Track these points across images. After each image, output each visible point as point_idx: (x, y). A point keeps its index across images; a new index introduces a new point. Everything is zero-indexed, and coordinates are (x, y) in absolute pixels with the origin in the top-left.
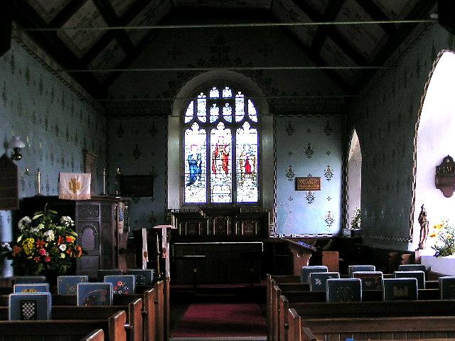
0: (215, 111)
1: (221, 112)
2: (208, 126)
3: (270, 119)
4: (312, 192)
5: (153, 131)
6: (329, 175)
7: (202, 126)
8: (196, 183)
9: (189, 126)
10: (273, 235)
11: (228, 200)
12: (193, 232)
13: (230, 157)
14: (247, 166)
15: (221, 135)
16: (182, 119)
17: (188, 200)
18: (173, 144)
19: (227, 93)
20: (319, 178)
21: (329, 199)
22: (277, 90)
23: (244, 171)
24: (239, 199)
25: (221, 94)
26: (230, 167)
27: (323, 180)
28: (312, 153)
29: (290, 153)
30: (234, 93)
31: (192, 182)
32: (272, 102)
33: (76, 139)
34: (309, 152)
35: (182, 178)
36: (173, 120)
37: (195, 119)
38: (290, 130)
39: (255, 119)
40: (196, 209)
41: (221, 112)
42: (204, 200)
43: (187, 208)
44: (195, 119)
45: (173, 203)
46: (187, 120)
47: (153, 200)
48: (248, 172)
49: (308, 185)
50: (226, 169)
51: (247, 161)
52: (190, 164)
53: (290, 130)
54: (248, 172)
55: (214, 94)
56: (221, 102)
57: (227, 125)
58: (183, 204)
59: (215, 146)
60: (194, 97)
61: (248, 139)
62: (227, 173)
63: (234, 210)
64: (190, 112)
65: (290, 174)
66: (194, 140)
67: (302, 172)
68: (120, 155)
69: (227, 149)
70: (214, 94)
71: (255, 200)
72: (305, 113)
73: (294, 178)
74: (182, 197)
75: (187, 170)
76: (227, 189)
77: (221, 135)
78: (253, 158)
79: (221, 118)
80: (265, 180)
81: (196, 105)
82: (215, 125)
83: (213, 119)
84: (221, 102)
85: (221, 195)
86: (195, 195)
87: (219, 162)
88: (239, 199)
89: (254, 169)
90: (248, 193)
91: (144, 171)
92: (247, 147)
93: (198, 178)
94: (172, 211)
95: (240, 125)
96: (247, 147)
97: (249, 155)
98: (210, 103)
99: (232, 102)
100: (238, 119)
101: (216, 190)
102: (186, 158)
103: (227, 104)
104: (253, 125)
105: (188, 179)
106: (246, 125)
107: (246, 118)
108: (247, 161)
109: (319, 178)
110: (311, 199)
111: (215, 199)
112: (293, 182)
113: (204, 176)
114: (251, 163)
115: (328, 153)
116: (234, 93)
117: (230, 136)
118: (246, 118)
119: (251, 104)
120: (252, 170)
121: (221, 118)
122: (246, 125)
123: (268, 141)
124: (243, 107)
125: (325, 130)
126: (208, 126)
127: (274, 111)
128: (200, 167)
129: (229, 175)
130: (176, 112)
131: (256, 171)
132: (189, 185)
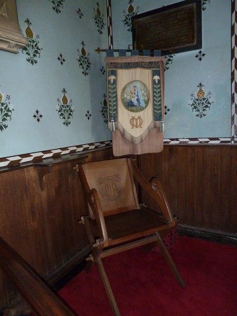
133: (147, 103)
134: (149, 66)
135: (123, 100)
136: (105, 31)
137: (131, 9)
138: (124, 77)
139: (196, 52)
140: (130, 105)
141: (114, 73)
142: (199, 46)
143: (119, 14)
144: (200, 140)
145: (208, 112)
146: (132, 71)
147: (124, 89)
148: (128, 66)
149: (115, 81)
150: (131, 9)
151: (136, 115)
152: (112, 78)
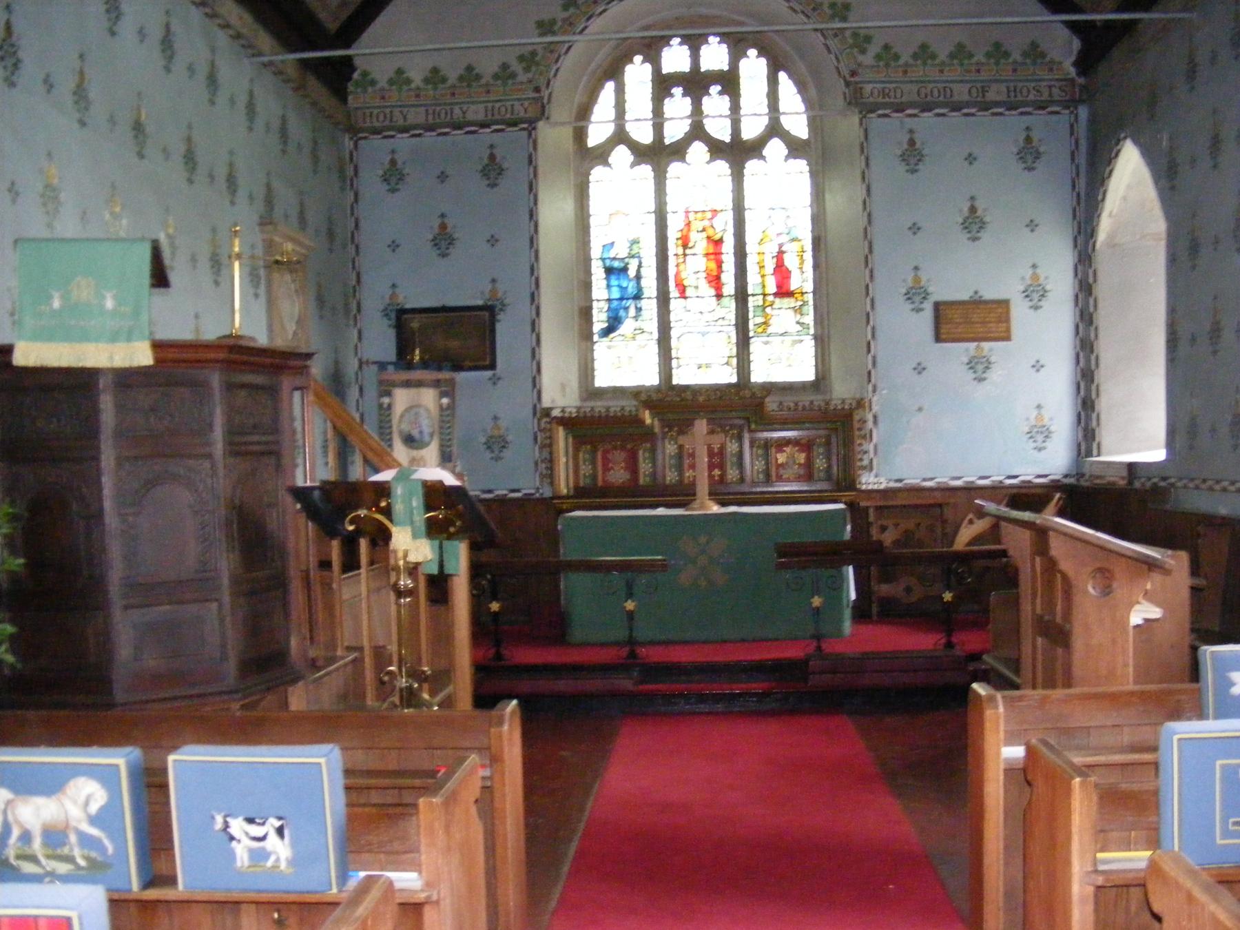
0: (678, 105)
1: (697, 110)
2: (659, 155)
3: (849, 126)
4: (986, 345)
5: (492, 170)
6: (1036, 293)
7: (642, 154)
8: (627, 326)
9: (601, 155)
10: (869, 481)
11: (727, 376)
12: (619, 475)
13: (728, 248)
14: (781, 271)
15: (699, 181)
17: (602, 380)
18: (554, 210)
19: (715, 56)
20: (1004, 304)
21: (1038, 366)
22: (868, 39)
23: (771, 287)
24: (759, 375)
26: (729, 278)
27: (1020, 312)
28: (982, 225)
29: (915, 229)
30: (736, 55)
32: (853, 73)
33: (231, 181)
34: (973, 223)
36: (553, 136)
37: (620, 137)
38: (912, 155)
39: (798, 125)
40: (629, 405)
41: (697, 110)
42: (650, 377)
43: (599, 406)
44: (620, 137)
45: (559, 391)
46: (597, 134)
47: (495, 380)
48: (784, 292)
49: (970, 322)
50: (715, 281)
51: (780, 256)
52: (609, 271)
53: (912, 155)
54: (784, 292)
55: (676, 58)
56: (696, 83)
57: (717, 149)
58: (591, 392)
59: (682, 216)
60: (614, 71)
61: (782, 194)
62: (719, 296)
63: (742, 406)
65: (916, 294)
66: (618, 204)
67: (952, 286)
68: (394, 246)
70: (676, 58)
71: (808, 375)
72: (956, 107)
73: (928, 307)
74: (587, 370)
75: (599, 289)
77: (699, 181)
78: (795, 246)
79: (697, 132)
80: (840, 312)
81: (620, 91)
82: (678, 151)
83: (675, 131)
84: (696, 83)
85: (704, 362)
86: (625, 364)
89: (803, 279)
90: (786, 356)
91: (465, 293)
93: (632, 312)
94: (556, 413)
95: (754, 149)
97: (784, 239)
98: (663, 85)
99: (729, 82)
102: (596, 252)
103: (715, 89)
104: (796, 148)
105: (604, 316)
106: (775, 148)
107: (775, 129)
108: (780, 256)
109: (1004, 304)
110: (979, 367)
112: (927, 316)
113: (650, 306)
114: (790, 262)
115: (1032, 225)
116: (736, 55)
117: (728, 183)
118: (775, 129)
119: (785, 83)
120: (794, 284)
121: (697, 132)
122: (775, 148)
123: (844, 201)
124: (764, 95)
125: (1021, 155)
126: (659, 155)
127: (858, 102)
128: (638, 277)
129: (725, 301)
130: (561, 111)
131: (809, 287)
133: (432, 435)
134: (436, 384)
135: (401, 432)
136: (352, 322)
137: (393, 295)
138: (401, 398)
139: (489, 373)
140: (410, 441)
141: (389, 394)
142: (492, 366)
143: (374, 298)
144: (497, 493)
145: (507, 453)
146: (413, 391)
147: (402, 416)
148: (407, 384)
149: (390, 406)
150: (393, 295)
151: (415, 453)
152: (386, 400)
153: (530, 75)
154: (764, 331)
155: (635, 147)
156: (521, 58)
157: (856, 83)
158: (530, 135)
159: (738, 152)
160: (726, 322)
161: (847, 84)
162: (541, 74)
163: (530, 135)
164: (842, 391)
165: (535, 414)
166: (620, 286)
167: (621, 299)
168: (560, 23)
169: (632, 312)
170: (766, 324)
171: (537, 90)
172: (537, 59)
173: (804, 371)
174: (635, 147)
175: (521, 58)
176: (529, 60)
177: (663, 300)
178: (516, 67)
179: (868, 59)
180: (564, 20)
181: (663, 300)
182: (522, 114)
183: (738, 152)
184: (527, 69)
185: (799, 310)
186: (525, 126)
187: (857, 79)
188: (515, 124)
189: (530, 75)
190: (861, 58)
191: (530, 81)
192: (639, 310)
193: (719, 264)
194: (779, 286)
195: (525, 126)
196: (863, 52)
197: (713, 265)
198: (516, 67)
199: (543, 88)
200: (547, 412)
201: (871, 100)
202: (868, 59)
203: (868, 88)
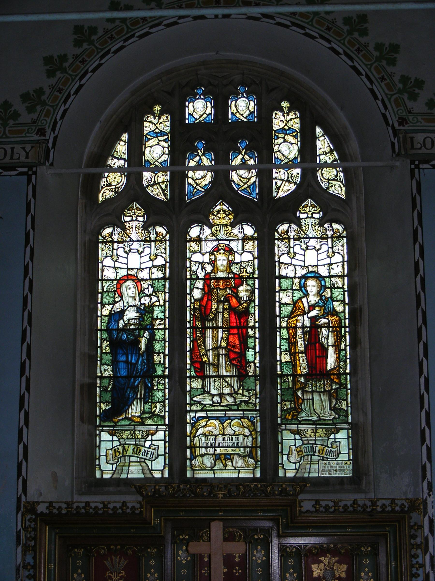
2: (176, 216)
8: (135, 410)
9: (113, 214)
15: (221, 248)
16: (92, 185)
22: (419, 84)
25: (221, 108)
31: (119, 405)
32: (402, 121)
35: (89, 390)
37: (134, 192)
44: (134, 192)
50: (238, 360)
51: (313, 331)
52: (116, 345)
54: (317, 371)
55: (199, 109)
56: (221, 136)
59: (200, 284)
62: (242, 376)
64: (113, 182)
69: (243, 291)
70: (199, 109)
76: (239, 432)
84: (221, 136)
87: (216, 338)
88: (289, 468)
92: (312, 286)
93: (141, 392)
96: (312, 286)
98: (183, 139)
99: (259, 137)
100: (284, 185)
101: (206, 431)
107: (309, 188)
108: (313, 331)
111: (203, 468)
114: (327, 337)
118: (309, 188)
121: (221, 189)
126: (176, 216)
129: (250, 383)
132: (107, 416)
153: (34, 116)
154: (295, 417)
155: (150, 205)
156: (25, 97)
157: (406, 132)
158: (29, 181)
159: (267, 215)
160: (251, 407)
161: (395, 133)
162: (47, 115)
163: (29, 181)
164: (392, 488)
165: (18, 508)
166: (126, 362)
167: (129, 377)
168: (71, 60)
169: (141, 392)
170: (297, 409)
171: (41, 132)
172: (44, 98)
173: (340, 467)
174: (150, 205)
175: (25, 97)
176: (33, 99)
177: (178, 378)
178: (19, 106)
179: (419, 106)
180: (76, 57)
181: (178, 378)
182: (23, 159)
183: (267, 215)
184: (31, 110)
185: (334, 396)
186: (25, 170)
187: (406, 128)
188: (13, 168)
189: (34, 116)
190: (410, 104)
191: (34, 122)
192: (149, 390)
193: (244, 339)
194: (310, 365)
195: (25, 170)
196: (413, 97)
197: (235, 340)
198: (19, 106)
199: (48, 131)
200: (31, 508)
201: (424, 151)
202: (419, 106)
203: (420, 137)
